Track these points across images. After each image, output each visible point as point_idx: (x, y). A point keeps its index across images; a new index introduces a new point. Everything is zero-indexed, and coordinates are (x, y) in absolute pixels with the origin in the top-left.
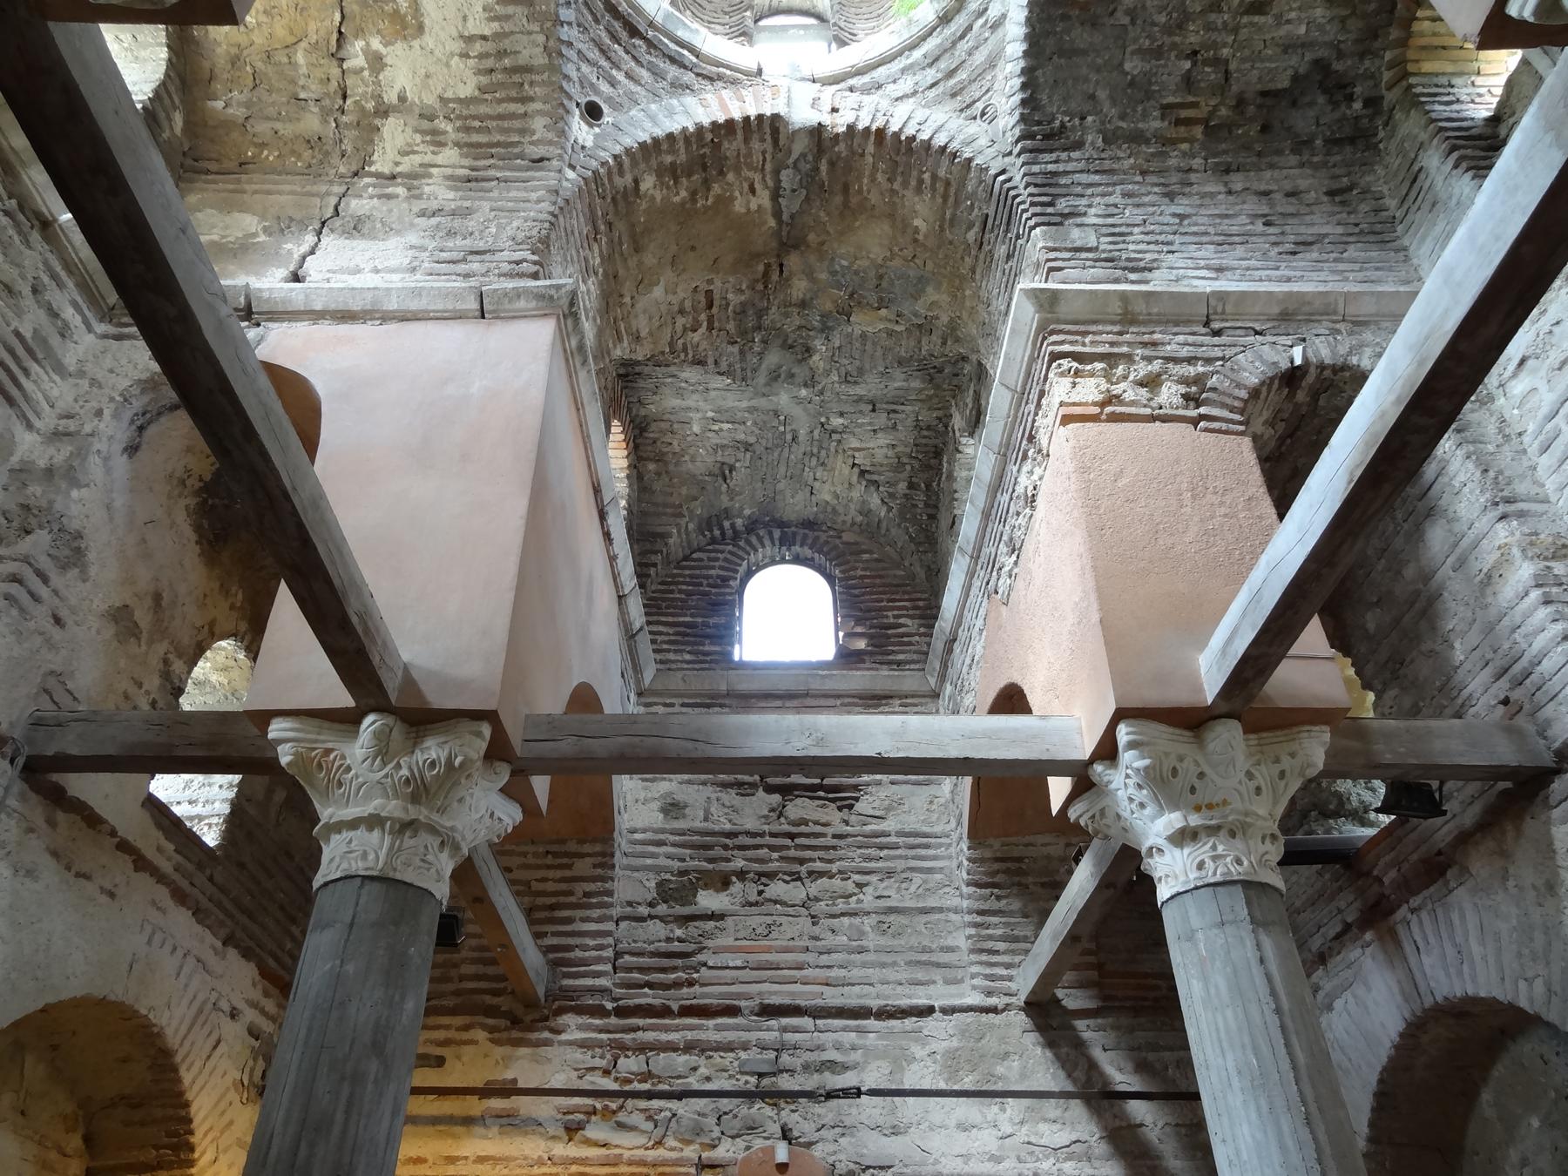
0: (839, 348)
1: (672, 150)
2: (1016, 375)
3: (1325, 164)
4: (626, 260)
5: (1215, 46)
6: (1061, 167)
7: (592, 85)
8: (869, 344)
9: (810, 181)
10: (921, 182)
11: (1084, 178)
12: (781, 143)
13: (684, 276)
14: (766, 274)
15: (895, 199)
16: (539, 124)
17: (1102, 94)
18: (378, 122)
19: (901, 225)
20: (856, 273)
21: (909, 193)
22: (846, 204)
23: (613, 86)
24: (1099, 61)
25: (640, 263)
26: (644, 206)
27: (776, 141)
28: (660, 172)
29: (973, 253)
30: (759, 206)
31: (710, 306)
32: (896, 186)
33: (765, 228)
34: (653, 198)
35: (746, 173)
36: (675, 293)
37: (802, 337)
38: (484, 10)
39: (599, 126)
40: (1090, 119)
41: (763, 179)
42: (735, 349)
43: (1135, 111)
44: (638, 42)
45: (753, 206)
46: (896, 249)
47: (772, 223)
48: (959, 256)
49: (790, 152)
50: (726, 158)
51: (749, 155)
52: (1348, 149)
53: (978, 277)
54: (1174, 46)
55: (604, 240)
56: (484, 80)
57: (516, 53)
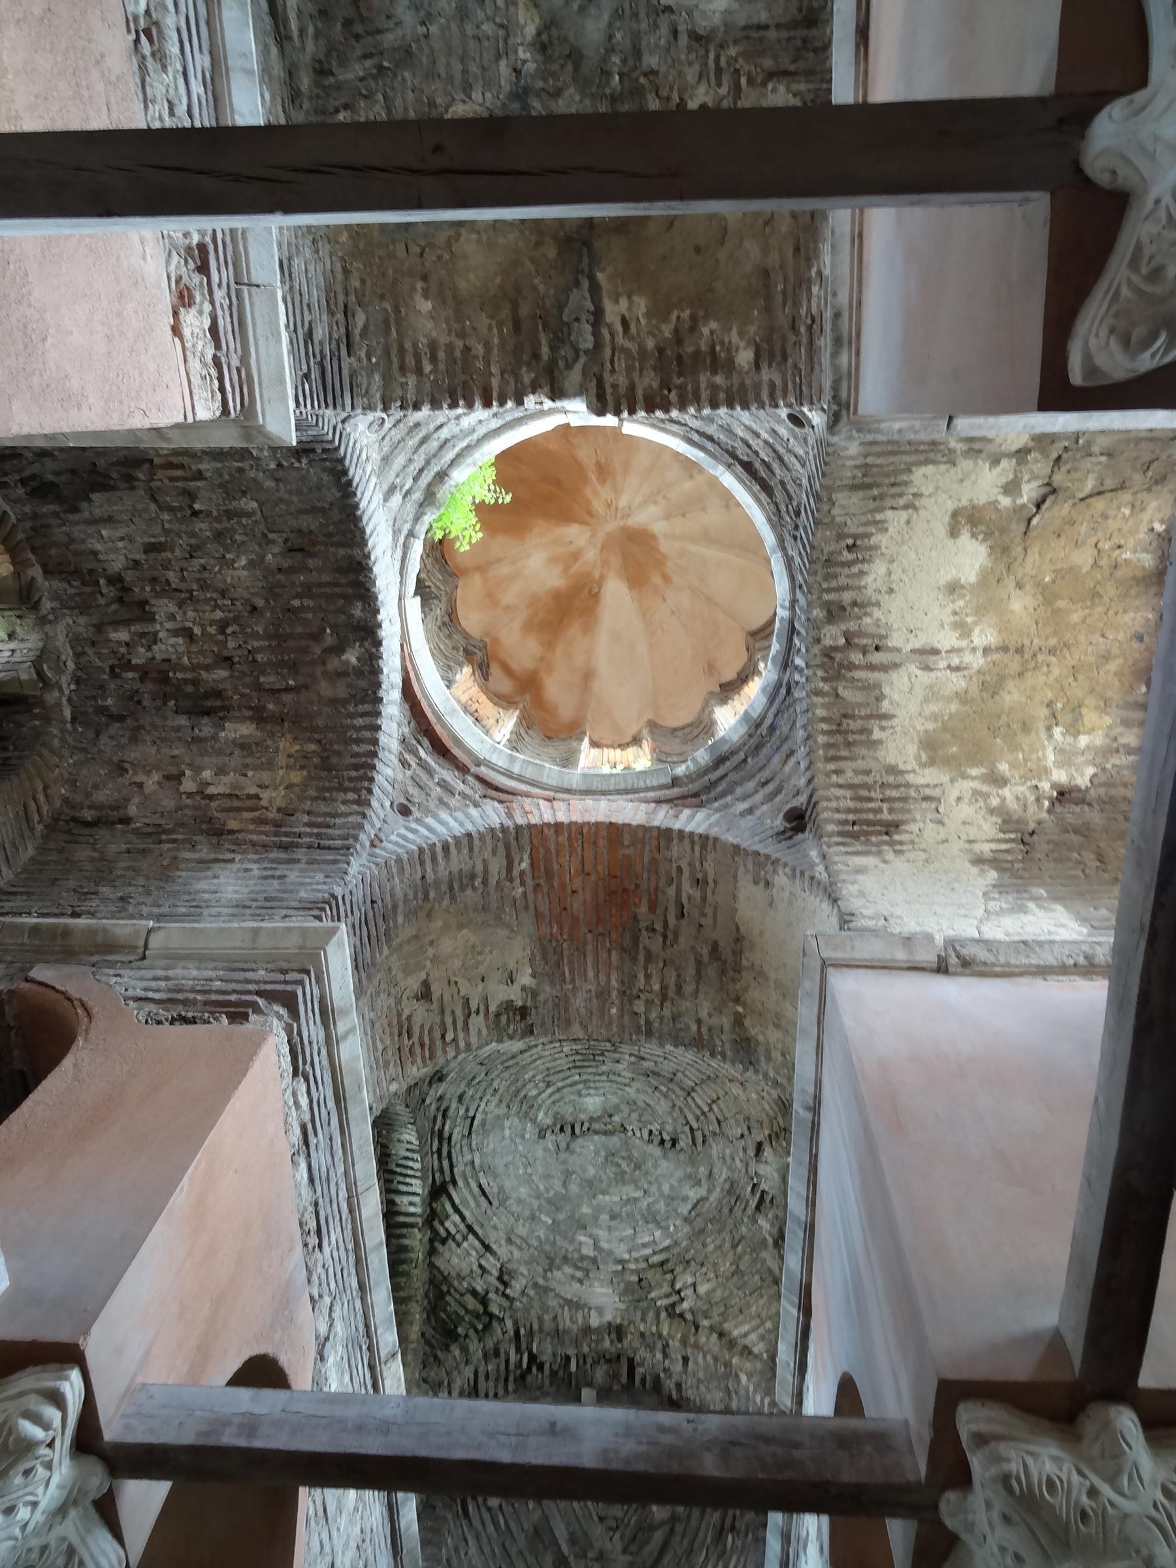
0: (498, 57)
1: (714, 388)
2: (257, 315)
4: (782, 266)
5: (180, 521)
7: (796, 438)
8: (458, 76)
9: (561, 335)
10: (433, 359)
12: (594, 383)
15: (456, 326)
17: (269, 484)
18: (1031, 444)
19: (444, 294)
21: (443, 339)
22: (515, 307)
23: (774, 431)
24: (283, 506)
25: (765, 250)
26: (752, 329)
28: (729, 366)
29: (353, 298)
30: (617, 302)
32: (459, 344)
33: (610, 269)
34: (741, 335)
35: (632, 346)
37: (554, 75)
38: (887, 530)
41: (612, 336)
42: (651, 60)
43: (230, 474)
44: (745, 458)
45: (624, 303)
46: (446, 256)
47: (600, 276)
48: (369, 283)
49: (584, 373)
50: (655, 368)
51: (629, 370)
53: (338, 267)
54: (217, 519)
55: (803, 311)
56: (905, 478)
57: (864, 499)
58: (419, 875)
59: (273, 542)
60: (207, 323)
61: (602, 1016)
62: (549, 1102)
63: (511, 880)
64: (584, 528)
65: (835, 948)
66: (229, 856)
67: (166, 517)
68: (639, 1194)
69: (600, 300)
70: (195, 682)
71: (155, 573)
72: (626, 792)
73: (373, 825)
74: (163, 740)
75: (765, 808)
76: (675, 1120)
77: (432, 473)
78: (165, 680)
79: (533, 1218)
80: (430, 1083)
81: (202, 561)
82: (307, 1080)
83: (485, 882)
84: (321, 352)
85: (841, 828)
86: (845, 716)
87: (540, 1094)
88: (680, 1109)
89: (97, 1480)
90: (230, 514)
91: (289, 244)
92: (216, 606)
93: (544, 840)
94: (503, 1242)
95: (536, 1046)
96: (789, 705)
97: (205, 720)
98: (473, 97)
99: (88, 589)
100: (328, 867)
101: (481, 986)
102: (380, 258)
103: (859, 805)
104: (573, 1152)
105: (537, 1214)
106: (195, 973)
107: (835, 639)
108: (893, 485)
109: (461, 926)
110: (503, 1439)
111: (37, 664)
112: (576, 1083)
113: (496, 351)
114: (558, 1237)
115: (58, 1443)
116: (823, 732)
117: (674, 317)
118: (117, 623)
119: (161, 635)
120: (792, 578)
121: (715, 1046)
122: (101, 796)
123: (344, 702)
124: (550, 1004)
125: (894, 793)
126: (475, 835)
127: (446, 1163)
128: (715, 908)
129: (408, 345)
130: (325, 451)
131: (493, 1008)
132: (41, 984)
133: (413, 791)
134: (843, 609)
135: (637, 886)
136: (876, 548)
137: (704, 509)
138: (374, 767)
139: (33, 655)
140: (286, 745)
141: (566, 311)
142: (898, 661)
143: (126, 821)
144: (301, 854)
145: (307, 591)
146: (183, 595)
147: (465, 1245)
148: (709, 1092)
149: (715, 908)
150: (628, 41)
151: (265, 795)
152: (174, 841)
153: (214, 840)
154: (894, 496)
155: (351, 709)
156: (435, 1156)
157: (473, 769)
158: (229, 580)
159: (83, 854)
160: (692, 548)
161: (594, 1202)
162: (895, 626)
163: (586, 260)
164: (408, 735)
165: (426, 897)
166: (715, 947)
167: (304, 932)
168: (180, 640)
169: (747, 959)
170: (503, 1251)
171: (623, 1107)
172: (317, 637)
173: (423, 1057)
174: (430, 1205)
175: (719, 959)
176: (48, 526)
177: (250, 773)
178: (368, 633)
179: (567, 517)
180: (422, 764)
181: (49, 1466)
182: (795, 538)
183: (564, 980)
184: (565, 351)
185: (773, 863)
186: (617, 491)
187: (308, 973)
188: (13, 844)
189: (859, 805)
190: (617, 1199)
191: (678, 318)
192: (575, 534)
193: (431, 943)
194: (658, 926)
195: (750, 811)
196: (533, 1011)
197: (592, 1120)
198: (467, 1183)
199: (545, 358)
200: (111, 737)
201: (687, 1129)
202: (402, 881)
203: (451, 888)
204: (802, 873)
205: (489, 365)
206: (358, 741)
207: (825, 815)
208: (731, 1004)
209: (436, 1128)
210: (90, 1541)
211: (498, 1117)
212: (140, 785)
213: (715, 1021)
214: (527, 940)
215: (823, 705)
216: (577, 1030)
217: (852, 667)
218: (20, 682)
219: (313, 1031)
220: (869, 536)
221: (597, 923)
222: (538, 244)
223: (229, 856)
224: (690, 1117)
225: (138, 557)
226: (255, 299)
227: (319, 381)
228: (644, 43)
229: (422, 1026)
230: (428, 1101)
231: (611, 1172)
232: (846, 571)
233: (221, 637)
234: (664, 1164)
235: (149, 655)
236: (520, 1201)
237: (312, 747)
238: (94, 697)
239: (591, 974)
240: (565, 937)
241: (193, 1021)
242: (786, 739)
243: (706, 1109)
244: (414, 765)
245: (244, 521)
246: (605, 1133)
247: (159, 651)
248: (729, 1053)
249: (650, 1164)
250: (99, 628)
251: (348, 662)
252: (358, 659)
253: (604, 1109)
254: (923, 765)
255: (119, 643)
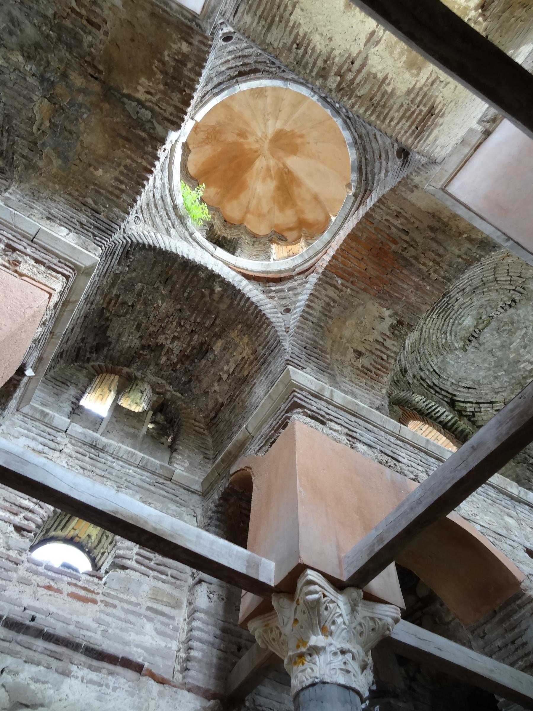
0: (25, 79)
1: (192, 70)
2: (46, 241)
3: (72, 347)
6: (115, 257)
7: (237, 43)
8: (24, 101)
9: (140, 124)
10: (122, 182)
11: (107, 266)
12: (166, 122)
13: (118, 23)
14: (95, 67)
15: (114, 165)
16: (248, 19)
17: (134, 274)
20: (76, 119)
21: (117, 173)
22: (120, 135)
23: (229, 52)
25: (143, 8)
26: (174, 36)
27: (168, 120)
28: (186, 57)
29: (80, 198)
30: (138, 91)
31: (89, 21)
32: (122, 168)
33: (124, 85)
34: (175, 43)
35: (159, 96)
36: (110, 9)
37: (41, 60)
38: (299, 23)
39: (221, 37)
40: (127, 269)
41: (151, 102)
42: (50, 13)
44: (236, 73)
45: (140, 88)
46: (87, 151)
47: (125, 91)
48: (79, 189)
49: (159, 123)
50: (172, 92)
51: (167, 103)
52: (75, 354)
53: (66, 196)
58: (311, 324)
59: (158, 287)
60: (33, 262)
61: (427, 294)
62: (453, 338)
63: (342, 291)
64: (260, 158)
65: (440, 179)
66: (253, 383)
67: (129, 316)
68: (524, 330)
69: (134, 98)
70: (194, 348)
71: (148, 333)
72: (346, 219)
73: (281, 327)
74: (206, 373)
75: (389, 164)
76: (504, 294)
77: (172, 211)
78: (188, 357)
79: (496, 378)
80: (404, 376)
81: (152, 315)
82: (331, 420)
83: (334, 301)
84: (91, 224)
85: (414, 136)
86: (371, 99)
87: (446, 339)
88: (500, 288)
89: (356, 593)
90: (139, 294)
91: (44, 210)
92: (171, 322)
93: (336, 267)
94: (495, 396)
95: (423, 327)
96: (355, 122)
97: (208, 354)
98: (35, 100)
99: (142, 358)
100: (279, 354)
101: (375, 331)
102: (73, 178)
103: (411, 120)
104: (484, 343)
105: (496, 375)
106: (267, 427)
107: (335, 81)
108: (278, 8)
109: (344, 323)
110: (459, 468)
111: (154, 391)
112: (454, 323)
113: (133, 155)
114: (513, 374)
115: (326, 593)
116: (371, 115)
117: (155, 69)
118: (159, 358)
119: (171, 346)
120: (302, 84)
121: (475, 257)
122: (211, 405)
123: (232, 303)
124: (405, 310)
125: (419, 98)
126: (313, 292)
127: (443, 393)
128: (413, 216)
129: (111, 189)
130: (131, 246)
131: (388, 333)
132: (235, 473)
133: (284, 302)
134: (324, 69)
135: (382, 242)
136: (305, 34)
137: (282, 100)
138: (261, 310)
139: (151, 391)
140: (233, 334)
141: (132, 115)
142: (365, 56)
143: (222, 405)
144: (270, 359)
145: (184, 287)
146: (161, 330)
147: (482, 409)
148: (503, 272)
149: (413, 216)
150: (39, 18)
151: (244, 355)
152: (237, 396)
153: (246, 383)
154: (285, 10)
155: (236, 303)
156: (437, 394)
157: (294, 274)
158: (164, 311)
159: (222, 426)
160: (296, 115)
161: (512, 350)
162: (348, 47)
163: (116, 93)
164: (263, 289)
165: (322, 327)
166: (431, 228)
167: (281, 381)
168: (176, 342)
169: (444, 218)
170: (498, 398)
171: (481, 311)
172: (203, 296)
173: (384, 372)
174: (454, 410)
175: (437, 229)
176: (111, 356)
177: (235, 354)
178: (213, 277)
179: (251, 163)
180: (277, 291)
181: (332, 602)
182: (284, 71)
183: (400, 298)
184: (148, 126)
185: (407, 178)
186: (253, 134)
187: (294, 391)
188: (203, 443)
189: (411, 120)
190: (519, 340)
191: (156, 67)
192: (260, 164)
193: (341, 338)
194: (405, 245)
195: (387, 172)
196: (403, 319)
197: (476, 327)
198: (459, 391)
199: (146, 136)
200: (195, 388)
201: (512, 292)
202: (307, 332)
203: (326, 315)
204: (418, 168)
205: (137, 162)
206: (248, 309)
207: (404, 139)
208: (460, 238)
209: (426, 386)
210: (375, 611)
211: (442, 361)
212: (215, 391)
213: (463, 250)
214: (372, 301)
215: (360, 107)
216: (424, 307)
217: (352, 81)
218: (156, 401)
219: (315, 405)
220: (298, 34)
221: (386, 269)
222: (101, 110)
223: (253, 383)
224: (508, 287)
225: (139, 335)
226: (40, 238)
227: (100, 232)
228: (42, 12)
229: (371, 364)
230: (411, 382)
231: (505, 335)
232: (308, 56)
233: (183, 328)
234: (520, 312)
235: (175, 355)
236: (484, 378)
237: (240, 326)
238: (179, 383)
239: (405, 286)
240: (382, 286)
241: (275, 440)
242: (368, 133)
243: (509, 278)
244: (275, 295)
245: (144, 292)
246: (487, 325)
247: (176, 351)
248: (482, 253)
249: (515, 317)
250: (157, 364)
251: (219, 292)
252: (220, 287)
253: (475, 319)
254: (418, 75)
255: (165, 362)
